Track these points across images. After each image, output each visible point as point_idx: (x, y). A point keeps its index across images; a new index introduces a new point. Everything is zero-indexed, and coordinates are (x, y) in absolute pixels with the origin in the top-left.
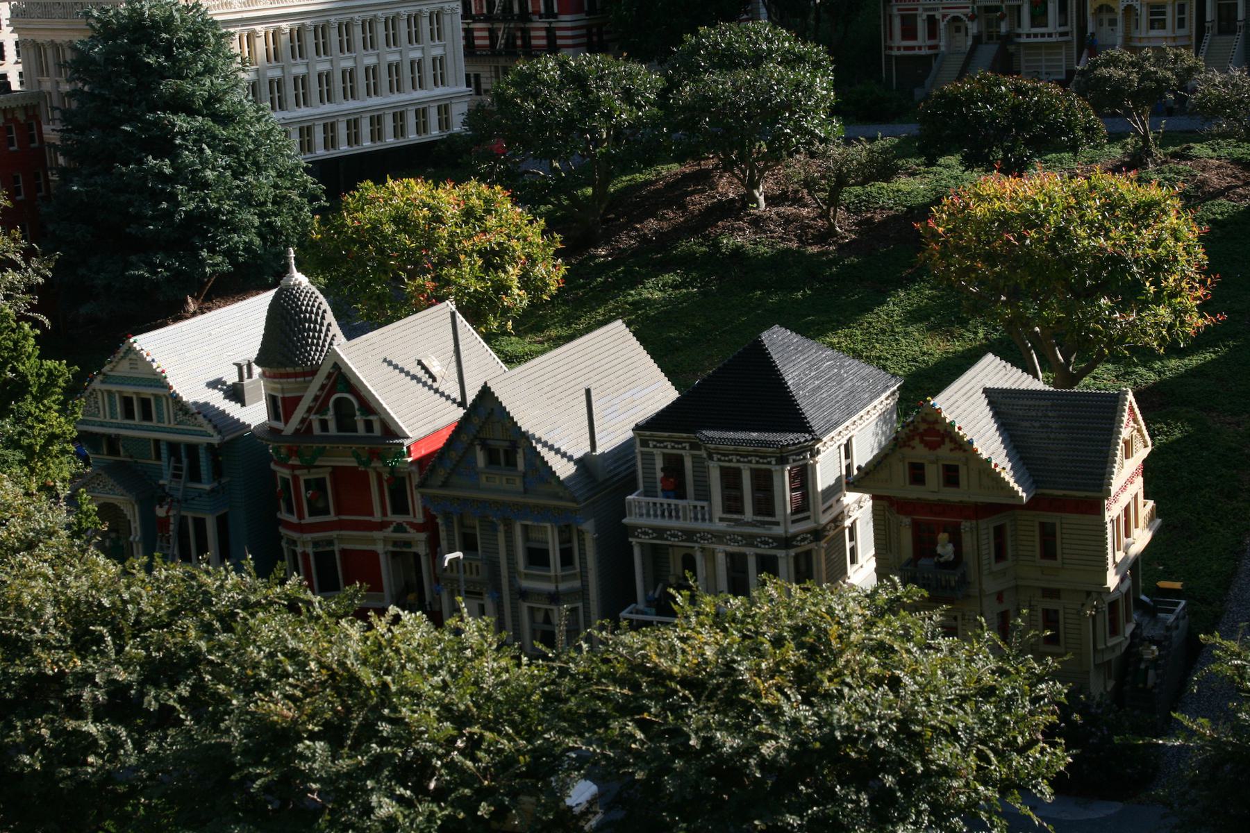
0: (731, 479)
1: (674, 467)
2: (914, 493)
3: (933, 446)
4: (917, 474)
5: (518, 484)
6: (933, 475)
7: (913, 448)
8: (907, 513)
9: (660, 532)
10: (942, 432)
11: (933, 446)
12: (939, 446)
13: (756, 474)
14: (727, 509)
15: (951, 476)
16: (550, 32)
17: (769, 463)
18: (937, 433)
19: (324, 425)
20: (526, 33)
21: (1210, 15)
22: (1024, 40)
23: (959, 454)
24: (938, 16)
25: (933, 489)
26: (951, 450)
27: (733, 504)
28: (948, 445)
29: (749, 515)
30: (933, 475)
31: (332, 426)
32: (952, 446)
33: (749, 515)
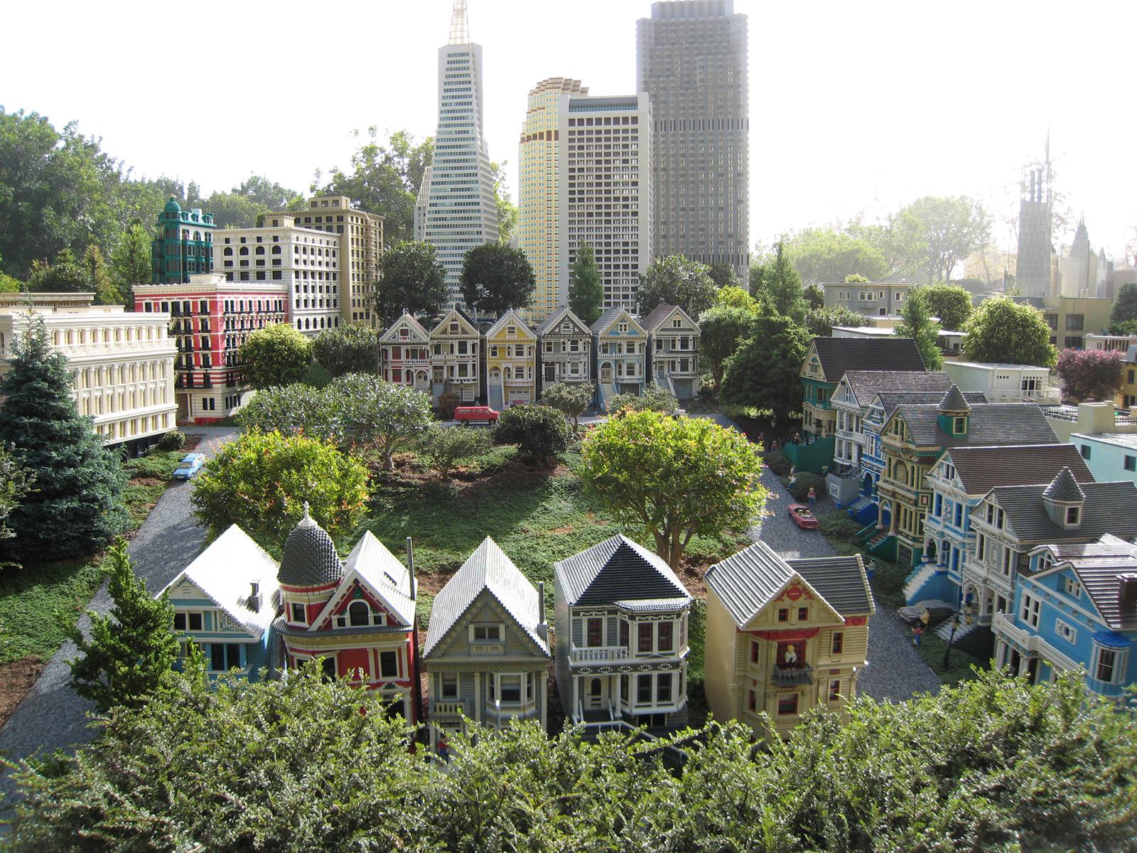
0: (645, 631)
1: (595, 626)
2: (783, 626)
3: (794, 598)
4: (783, 615)
5: (501, 649)
6: (794, 615)
8: (774, 639)
9: (595, 669)
11: (794, 598)
13: (661, 626)
14: (641, 649)
15: (803, 614)
16: (207, 377)
18: (798, 590)
19: (341, 622)
20: (190, 377)
21: (543, 373)
22: (455, 382)
23: (809, 601)
24: (413, 370)
25: (794, 623)
27: (645, 645)
29: (655, 651)
30: (794, 615)
31: (348, 622)
33: (655, 651)
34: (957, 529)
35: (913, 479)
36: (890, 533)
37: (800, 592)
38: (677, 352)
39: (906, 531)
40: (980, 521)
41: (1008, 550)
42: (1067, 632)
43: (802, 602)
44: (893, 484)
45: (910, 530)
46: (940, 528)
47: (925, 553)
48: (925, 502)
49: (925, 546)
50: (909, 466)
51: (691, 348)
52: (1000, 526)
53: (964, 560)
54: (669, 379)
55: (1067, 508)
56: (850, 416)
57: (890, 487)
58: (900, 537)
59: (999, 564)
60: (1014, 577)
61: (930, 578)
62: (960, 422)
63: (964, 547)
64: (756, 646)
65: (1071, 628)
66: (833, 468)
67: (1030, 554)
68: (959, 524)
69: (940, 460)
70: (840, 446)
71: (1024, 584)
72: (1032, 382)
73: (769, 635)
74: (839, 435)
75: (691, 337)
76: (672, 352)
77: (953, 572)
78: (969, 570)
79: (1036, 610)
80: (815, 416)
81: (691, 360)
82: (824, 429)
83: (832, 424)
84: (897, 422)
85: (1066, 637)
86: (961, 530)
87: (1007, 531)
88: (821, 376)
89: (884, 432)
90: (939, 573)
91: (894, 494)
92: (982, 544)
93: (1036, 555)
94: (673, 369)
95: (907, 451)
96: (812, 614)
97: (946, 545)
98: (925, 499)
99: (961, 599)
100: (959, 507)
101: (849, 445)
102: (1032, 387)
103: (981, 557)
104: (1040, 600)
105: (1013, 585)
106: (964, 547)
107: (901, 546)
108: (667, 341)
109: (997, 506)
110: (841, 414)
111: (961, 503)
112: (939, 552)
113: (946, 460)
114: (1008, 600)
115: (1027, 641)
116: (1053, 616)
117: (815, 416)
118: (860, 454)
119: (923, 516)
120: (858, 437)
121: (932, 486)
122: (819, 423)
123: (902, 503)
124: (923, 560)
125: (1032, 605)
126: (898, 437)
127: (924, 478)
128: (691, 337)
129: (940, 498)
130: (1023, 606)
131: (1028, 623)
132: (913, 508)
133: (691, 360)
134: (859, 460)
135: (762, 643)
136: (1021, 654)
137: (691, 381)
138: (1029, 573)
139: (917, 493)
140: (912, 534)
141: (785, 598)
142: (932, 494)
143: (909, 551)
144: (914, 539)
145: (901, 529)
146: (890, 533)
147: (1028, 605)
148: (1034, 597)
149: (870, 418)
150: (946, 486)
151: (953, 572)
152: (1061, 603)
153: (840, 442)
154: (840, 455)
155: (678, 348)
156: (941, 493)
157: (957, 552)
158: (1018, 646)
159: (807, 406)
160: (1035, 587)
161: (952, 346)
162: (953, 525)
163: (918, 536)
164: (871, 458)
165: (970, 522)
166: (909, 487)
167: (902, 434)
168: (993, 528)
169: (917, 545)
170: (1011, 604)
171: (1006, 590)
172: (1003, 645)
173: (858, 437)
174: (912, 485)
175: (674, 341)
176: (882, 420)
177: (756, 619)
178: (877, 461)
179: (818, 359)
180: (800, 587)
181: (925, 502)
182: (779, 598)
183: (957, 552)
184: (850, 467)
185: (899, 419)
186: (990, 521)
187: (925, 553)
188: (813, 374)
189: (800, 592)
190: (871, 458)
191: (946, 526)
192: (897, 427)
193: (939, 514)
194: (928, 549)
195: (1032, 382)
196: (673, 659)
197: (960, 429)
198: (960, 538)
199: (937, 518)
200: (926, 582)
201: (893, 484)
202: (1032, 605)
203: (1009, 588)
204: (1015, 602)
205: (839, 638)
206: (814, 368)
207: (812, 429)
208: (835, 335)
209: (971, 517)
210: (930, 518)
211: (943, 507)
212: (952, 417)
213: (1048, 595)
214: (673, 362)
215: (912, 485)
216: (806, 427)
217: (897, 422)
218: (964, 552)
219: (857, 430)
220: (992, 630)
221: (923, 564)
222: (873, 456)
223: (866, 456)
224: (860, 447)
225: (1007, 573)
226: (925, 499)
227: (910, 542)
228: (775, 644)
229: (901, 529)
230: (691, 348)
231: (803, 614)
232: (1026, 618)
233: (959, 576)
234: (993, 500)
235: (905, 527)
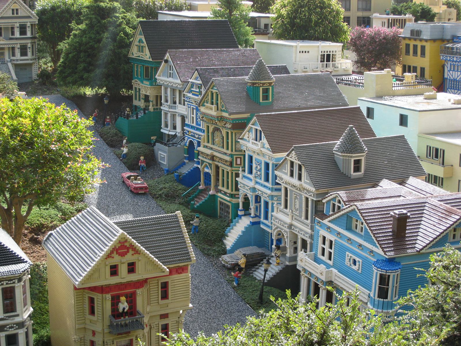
4: (114, 271)
6: (123, 269)
7: (113, 257)
8: (107, 292)
10: (128, 246)
11: (123, 255)
12: (126, 254)
17: (14, 283)
23: (136, 256)
26: (133, 255)
28: (131, 252)
30: (123, 269)
32: (133, 252)
34: (266, 184)
35: (228, 143)
36: (211, 192)
37: (128, 249)
38: (17, 39)
39: (225, 189)
40: (284, 176)
41: (307, 199)
42: (355, 262)
43: (130, 257)
44: (212, 149)
45: (228, 188)
46: (251, 184)
47: (241, 207)
48: (239, 162)
49: (241, 201)
50: (224, 132)
51: (29, 34)
52: (300, 178)
53: (273, 211)
54: (10, 64)
55: (353, 160)
56: (173, 90)
57: (209, 152)
58: (219, 195)
59: (301, 212)
60: (313, 221)
61: (246, 228)
62: (266, 91)
63: (272, 199)
64: (92, 301)
65: (357, 259)
66: (161, 138)
67: (324, 201)
68: (267, 180)
69: (250, 125)
70: (166, 118)
71: (321, 226)
72: (328, 56)
73: (102, 290)
74: (165, 108)
75: (29, 24)
76: (11, 39)
77: (265, 221)
78: (277, 218)
79: (331, 248)
80: (143, 92)
81: (29, 45)
82: (151, 104)
83: (158, 98)
84: (212, 94)
85: (354, 267)
86: (269, 185)
87: (306, 183)
88: (146, 55)
89: (201, 103)
90: (253, 224)
91: (213, 158)
92: (286, 195)
93: (329, 201)
94: (14, 55)
95: (221, 119)
96: (139, 267)
97: (258, 199)
98: (239, 160)
99: (272, 244)
100: (267, 165)
101: (174, 116)
102: (328, 60)
103: (286, 207)
104: (333, 238)
105: (312, 228)
106: (272, 199)
107: (221, 203)
108: (6, 29)
109: (297, 162)
110: (166, 89)
111: (268, 161)
112: (252, 206)
113: (254, 125)
114: (309, 241)
115: (324, 274)
116: (343, 250)
117: (143, 92)
118: (183, 124)
119: (237, 175)
120: (181, 109)
121: (244, 148)
122: (147, 98)
123: (220, 165)
124: (240, 213)
125: (327, 243)
126: (214, 107)
127: (237, 142)
128: (29, 24)
129: (251, 158)
130: (320, 245)
131: (325, 258)
132: (229, 169)
133: (29, 45)
134: (183, 130)
135: (97, 297)
136: (320, 285)
137: (30, 65)
138: (323, 216)
139: (231, 156)
140: (229, 191)
141: (115, 255)
142: (244, 156)
143: (228, 207)
144: (232, 196)
145: (220, 187)
146: (211, 192)
147: (324, 243)
148: (329, 237)
149: (190, 91)
150: (255, 147)
151: (265, 221)
152: (349, 239)
153: (166, 114)
154: (167, 126)
155: (17, 34)
156: (251, 154)
157: (266, 203)
158: (317, 278)
159: (136, 83)
160: (329, 228)
161: (262, 26)
162: (262, 181)
163: (234, 192)
164: (192, 127)
165: (276, 176)
166: (225, 150)
167: (217, 104)
168: (295, 181)
169: (234, 201)
170: (311, 244)
171: (307, 233)
172: (306, 279)
173: (181, 109)
174: (228, 149)
175: (13, 28)
176: (200, 93)
177: (90, 276)
178: (198, 129)
179: (144, 40)
180: (127, 244)
181: (239, 162)
182: (109, 256)
183: (266, 203)
184: (175, 136)
185: (214, 91)
186: (292, 175)
187: (241, 207)
188: (140, 54)
189: (128, 249)
190: (192, 127)
191: (257, 183)
192: (212, 98)
193: (251, 172)
194: (243, 203)
195: (328, 56)
196: (18, 320)
197: (266, 98)
198: (269, 192)
199: (250, 176)
200: (243, 232)
201: (212, 149)
202: (327, 243)
203: (309, 231)
204: (314, 242)
205: (165, 286)
206: (141, 49)
207: (141, 104)
208: (161, 18)
209: (276, 172)
210: (244, 177)
211: (254, 166)
212: (259, 87)
213: (339, 234)
214: (13, 49)
215: (228, 149)
216: (136, 103)
217: (212, 94)
218: (273, 204)
219: (180, 103)
220: (298, 267)
221: (240, 217)
222: (194, 125)
223: (188, 126)
224: (183, 118)
225: (307, 218)
226: (239, 160)
227: (228, 199)
228: (108, 296)
229: (220, 187)
230: (29, 34)
231: (132, 268)
232: (323, 254)
233: (269, 224)
234: (293, 157)
235: (223, 186)
